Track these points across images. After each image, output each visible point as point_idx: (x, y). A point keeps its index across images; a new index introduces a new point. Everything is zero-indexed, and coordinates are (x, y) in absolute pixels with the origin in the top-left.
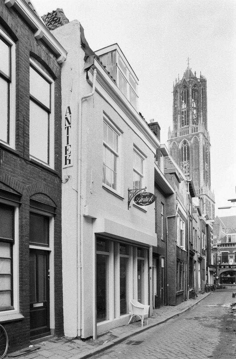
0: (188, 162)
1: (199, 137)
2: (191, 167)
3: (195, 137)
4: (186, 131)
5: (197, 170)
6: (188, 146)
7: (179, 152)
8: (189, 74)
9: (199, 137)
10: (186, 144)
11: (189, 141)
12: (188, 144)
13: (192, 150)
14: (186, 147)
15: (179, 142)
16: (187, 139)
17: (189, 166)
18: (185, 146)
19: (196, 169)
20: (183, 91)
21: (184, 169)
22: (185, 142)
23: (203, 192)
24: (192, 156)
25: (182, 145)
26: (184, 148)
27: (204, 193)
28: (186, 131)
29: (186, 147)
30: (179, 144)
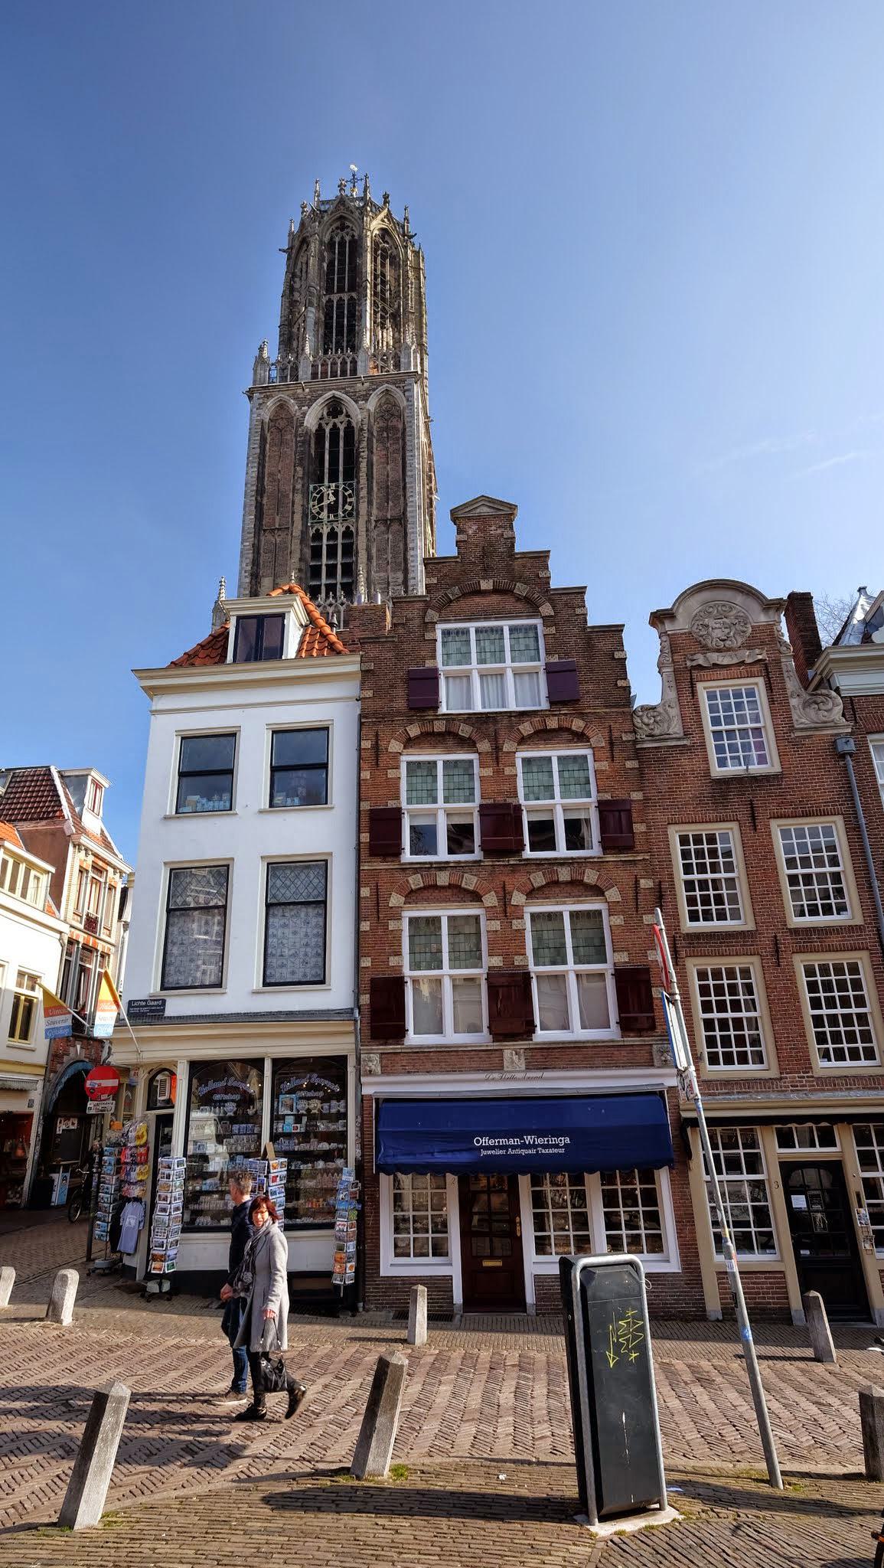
0: (351, 486)
2: (363, 507)
4: (344, 363)
5: (395, 527)
6: (349, 422)
7: (306, 442)
10: (342, 418)
11: (356, 402)
12: (348, 416)
13: (370, 441)
14: (342, 427)
16: (346, 393)
17: (350, 504)
18: (335, 425)
19: (386, 522)
20: (332, 238)
21: (324, 514)
22: (335, 408)
24: (370, 465)
26: (327, 431)
28: (344, 363)
29: (342, 427)
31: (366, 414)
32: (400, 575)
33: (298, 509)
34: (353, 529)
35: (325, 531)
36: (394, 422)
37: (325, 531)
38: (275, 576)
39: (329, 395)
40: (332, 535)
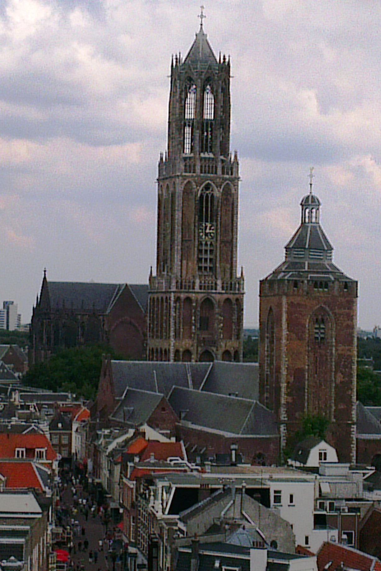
1: (234, 186)
3: (228, 184)
4: (212, 167)
8: (200, 46)
9: (234, 186)
11: (217, 187)
14: (210, 196)
15: (198, 184)
16: (214, 183)
22: (207, 187)
23: (241, 289)
25: (202, 190)
27: (242, 292)
28: (212, 167)
29: (210, 196)
30: (198, 188)
31: (220, 195)
32: (229, 266)
33: (196, 235)
34: (213, 243)
35: (204, 243)
36: (229, 197)
37: (204, 243)
38: (187, 260)
39: (207, 182)
40: (206, 244)
